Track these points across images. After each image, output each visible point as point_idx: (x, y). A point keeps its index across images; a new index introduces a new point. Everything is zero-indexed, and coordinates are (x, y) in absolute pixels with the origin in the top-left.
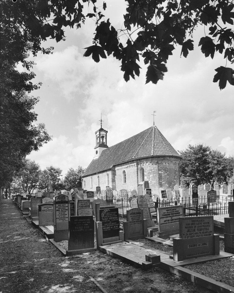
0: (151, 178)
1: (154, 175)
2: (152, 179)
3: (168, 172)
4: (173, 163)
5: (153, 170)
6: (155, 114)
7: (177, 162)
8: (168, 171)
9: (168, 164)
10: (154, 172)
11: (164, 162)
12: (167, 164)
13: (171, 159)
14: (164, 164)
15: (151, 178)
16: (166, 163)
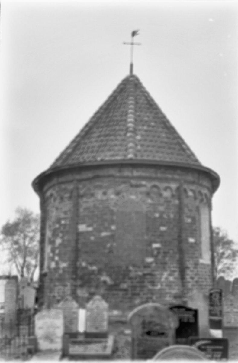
0: (57, 251)
1: (66, 238)
2: (59, 255)
3: (113, 227)
4: (143, 189)
5: (63, 222)
6: (136, 39)
7: (163, 185)
8: (112, 222)
9: (118, 194)
10: (65, 225)
11: (100, 187)
12: (113, 196)
13: (127, 173)
14: (99, 195)
15: (57, 251)
16: (105, 193)
